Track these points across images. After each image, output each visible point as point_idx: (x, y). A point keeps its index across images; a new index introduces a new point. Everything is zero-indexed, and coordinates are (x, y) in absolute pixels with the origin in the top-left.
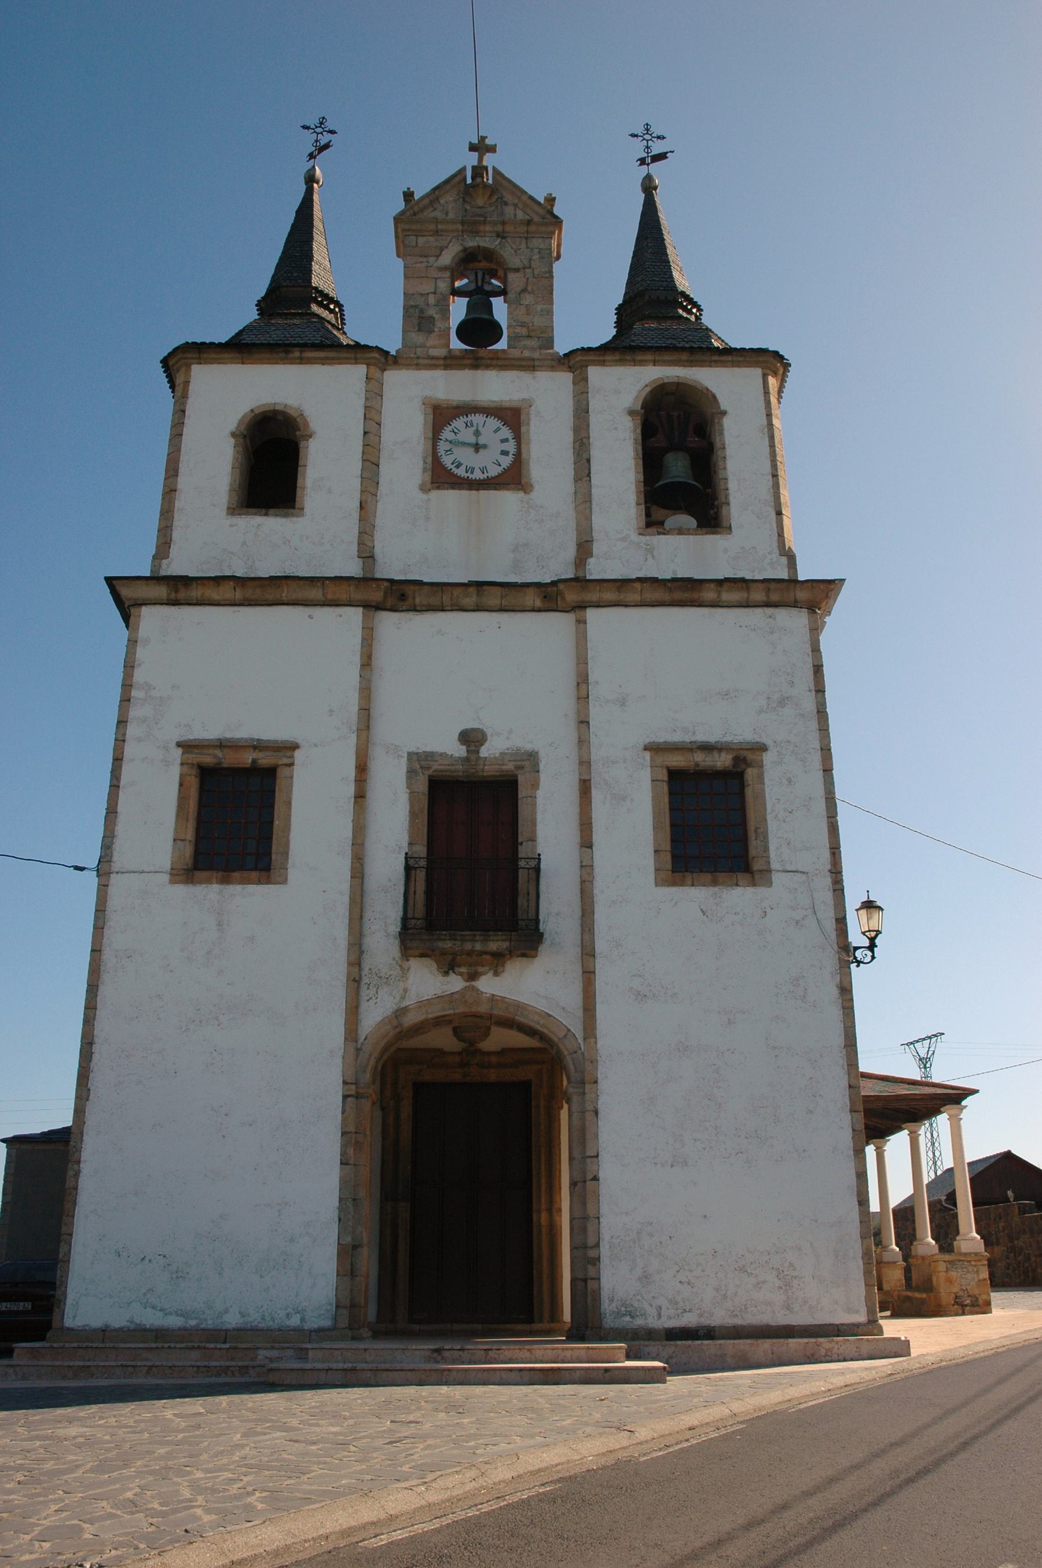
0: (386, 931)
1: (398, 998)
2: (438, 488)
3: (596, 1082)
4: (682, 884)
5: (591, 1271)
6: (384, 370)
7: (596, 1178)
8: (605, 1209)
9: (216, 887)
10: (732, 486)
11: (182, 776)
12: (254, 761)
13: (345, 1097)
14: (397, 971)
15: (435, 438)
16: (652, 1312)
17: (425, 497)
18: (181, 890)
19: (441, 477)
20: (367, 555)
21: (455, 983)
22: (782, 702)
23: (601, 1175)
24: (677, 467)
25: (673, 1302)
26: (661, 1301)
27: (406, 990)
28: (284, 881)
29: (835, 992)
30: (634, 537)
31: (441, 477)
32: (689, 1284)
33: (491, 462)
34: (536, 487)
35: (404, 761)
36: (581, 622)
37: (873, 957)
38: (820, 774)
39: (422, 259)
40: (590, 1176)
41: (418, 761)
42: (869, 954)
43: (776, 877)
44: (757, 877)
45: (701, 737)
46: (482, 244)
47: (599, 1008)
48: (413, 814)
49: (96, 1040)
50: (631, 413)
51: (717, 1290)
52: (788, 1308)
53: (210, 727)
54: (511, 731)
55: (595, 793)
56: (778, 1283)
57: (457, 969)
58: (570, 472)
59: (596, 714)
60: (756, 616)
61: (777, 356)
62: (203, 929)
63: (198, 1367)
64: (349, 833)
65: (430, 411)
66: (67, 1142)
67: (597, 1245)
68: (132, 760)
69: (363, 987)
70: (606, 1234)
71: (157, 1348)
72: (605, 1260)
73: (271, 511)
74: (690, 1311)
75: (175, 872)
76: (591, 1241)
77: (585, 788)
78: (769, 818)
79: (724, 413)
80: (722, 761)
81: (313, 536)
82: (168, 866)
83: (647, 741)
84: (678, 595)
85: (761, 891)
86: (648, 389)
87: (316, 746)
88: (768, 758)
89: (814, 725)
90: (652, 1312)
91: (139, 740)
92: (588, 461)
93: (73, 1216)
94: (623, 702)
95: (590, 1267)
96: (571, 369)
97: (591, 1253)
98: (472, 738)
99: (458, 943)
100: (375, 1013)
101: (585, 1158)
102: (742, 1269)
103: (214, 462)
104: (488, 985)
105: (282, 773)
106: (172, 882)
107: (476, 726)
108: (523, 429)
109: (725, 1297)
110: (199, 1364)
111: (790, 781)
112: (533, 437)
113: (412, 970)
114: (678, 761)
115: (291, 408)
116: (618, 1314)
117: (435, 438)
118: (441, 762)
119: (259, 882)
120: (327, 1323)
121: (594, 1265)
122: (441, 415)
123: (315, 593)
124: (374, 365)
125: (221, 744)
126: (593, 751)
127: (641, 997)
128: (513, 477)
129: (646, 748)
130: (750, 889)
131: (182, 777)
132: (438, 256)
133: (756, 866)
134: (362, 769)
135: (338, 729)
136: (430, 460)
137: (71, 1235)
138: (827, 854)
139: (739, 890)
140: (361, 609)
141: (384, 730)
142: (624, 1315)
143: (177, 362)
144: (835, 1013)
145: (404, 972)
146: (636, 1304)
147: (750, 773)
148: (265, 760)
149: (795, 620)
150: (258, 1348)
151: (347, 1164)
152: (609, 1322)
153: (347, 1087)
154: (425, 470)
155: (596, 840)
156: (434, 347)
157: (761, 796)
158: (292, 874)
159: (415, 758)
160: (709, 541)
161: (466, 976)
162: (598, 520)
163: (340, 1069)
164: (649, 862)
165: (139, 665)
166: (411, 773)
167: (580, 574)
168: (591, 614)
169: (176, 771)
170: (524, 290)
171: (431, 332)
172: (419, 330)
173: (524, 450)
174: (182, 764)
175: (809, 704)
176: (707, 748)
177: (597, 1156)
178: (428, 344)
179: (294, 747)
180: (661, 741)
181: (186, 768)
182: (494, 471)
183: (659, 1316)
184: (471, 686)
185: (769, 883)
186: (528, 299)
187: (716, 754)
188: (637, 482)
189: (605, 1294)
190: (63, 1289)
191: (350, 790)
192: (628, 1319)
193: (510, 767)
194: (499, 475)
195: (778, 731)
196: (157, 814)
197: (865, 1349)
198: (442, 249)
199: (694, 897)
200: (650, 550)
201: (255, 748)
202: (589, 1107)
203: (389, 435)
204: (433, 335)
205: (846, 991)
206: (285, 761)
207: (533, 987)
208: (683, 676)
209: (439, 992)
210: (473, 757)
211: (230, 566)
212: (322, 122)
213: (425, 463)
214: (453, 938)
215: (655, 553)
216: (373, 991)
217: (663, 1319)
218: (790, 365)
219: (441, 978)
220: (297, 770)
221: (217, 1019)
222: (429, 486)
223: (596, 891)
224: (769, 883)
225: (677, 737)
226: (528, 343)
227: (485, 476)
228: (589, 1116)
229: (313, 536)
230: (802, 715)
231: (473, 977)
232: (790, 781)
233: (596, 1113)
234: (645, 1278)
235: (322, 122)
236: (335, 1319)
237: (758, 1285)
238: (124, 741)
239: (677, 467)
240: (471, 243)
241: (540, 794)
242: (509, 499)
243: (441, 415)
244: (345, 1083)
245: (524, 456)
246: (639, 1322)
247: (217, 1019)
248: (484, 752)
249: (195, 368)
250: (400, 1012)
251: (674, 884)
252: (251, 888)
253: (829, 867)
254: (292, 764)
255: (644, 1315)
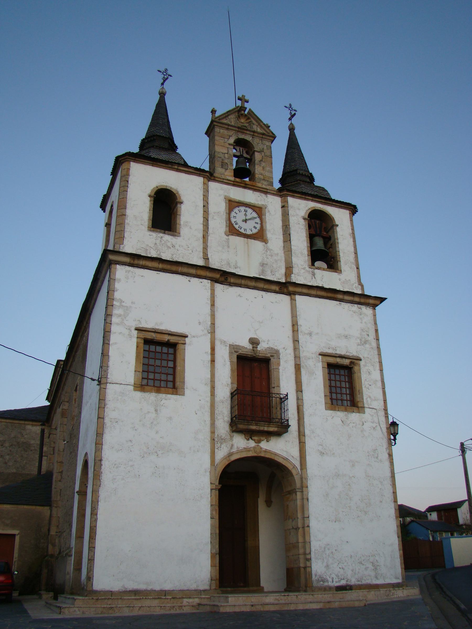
0: (223, 419)
1: (229, 448)
2: (232, 235)
3: (307, 487)
4: (335, 410)
5: (308, 564)
6: (209, 181)
7: (308, 526)
8: (312, 538)
9: (154, 394)
10: (341, 254)
11: (137, 343)
12: (168, 340)
13: (211, 489)
14: (229, 437)
15: (229, 214)
16: (330, 580)
17: (227, 237)
18: (139, 394)
19: (233, 230)
20: (206, 258)
21: (252, 444)
22: (366, 342)
23: (310, 525)
24: (320, 243)
25: (337, 576)
26: (333, 576)
27: (232, 445)
28: (183, 394)
29: (387, 456)
30: (307, 268)
31: (233, 230)
32: (343, 568)
33: (250, 227)
34: (269, 242)
35: (228, 347)
36: (293, 300)
37: (395, 443)
38: (379, 371)
39: (222, 139)
40: (306, 525)
41: (233, 348)
42: (394, 442)
43: (367, 410)
44: (360, 409)
45: (339, 352)
46: (245, 138)
47: (308, 457)
48: (232, 370)
49: (103, 459)
50: (304, 219)
51: (352, 571)
52: (376, 577)
53: (150, 323)
54: (268, 341)
55: (302, 370)
56: (373, 568)
57: (253, 438)
58: (281, 237)
59: (301, 338)
60: (355, 307)
61: (355, 207)
62: (149, 412)
63: (161, 607)
64: (209, 376)
65: (227, 202)
66: (47, 501)
67: (310, 553)
68: (115, 333)
69: (216, 443)
70: (313, 549)
71: (140, 599)
72: (313, 560)
73: (167, 232)
74: (343, 579)
75: (136, 386)
76: (307, 552)
77: (213, 361)
78: (363, 386)
79: (337, 225)
80: (346, 362)
81: (183, 246)
82: (132, 381)
83: (320, 351)
84: (329, 295)
85: (362, 415)
86: (310, 211)
87: (194, 337)
88: (362, 363)
89: (376, 352)
90: (330, 580)
91: (118, 324)
92: (290, 235)
93: (95, 539)
94: (310, 334)
95: (307, 562)
96: (281, 196)
97: (308, 557)
98: (254, 342)
99: (258, 427)
100: (221, 454)
101: (304, 518)
102: (361, 563)
103: (139, 207)
104: (264, 445)
105: (180, 347)
106: (135, 390)
107: (256, 337)
108: (263, 217)
109: (355, 574)
110: (162, 605)
111: (369, 373)
112: (267, 221)
113: (234, 437)
114: (331, 360)
115: (173, 189)
116: (318, 581)
117: (229, 214)
118: (242, 350)
119: (173, 394)
120: (207, 587)
121: (309, 561)
122: (232, 204)
123: (193, 271)
124: (206, 178)
125: (155, 331)
126: (301, 353)
127: (322, 454)
128: (260, 236)
129: (320, 355)
130: (358, 414)
131: (137, 343)
132: (228, 139)
133: (360, 405)
134: (213, 349)
135: (203, 331)
136: (228, 222)
137: (94, 548)
138: (382, 403)
139: (354, 414)
140: (210, 281)
141: (219, 334)
142: (320, 581)
143: (122, 160)
144: (387, 464)
145: (232, 437)
146: (324, 577)
147: (356, 368)
148: (173, 339)
149: (368, 311)
150: (184, 598)
151: (213, 518)
152: (315, 584)
153: (212, 485)
154: (226, 226)
155: (302, 388)
156: (228, 176)
157: (360, 378)
158: (187, 392)
159: (232, 347)
160: (333, 275)
161: (256, 441)
162: (294, 260)
163: (209, 477)
164: (323, 400)
165: (117, 291)
166: (231, 353)
167: (288, 280)
168: (298, 297)
169: (135, 340)
170: (261, 161)
171: (227, 169)
172: (222, 167)
173: (264, 226)
174: (137, 338)
175: (374, 344)
176: (341, 357)
177: (308, 517)
178: (226, 174)
179: (186, 337)
180: (325, 352)
181: (139, 340)
182: (249, 232)
183: (333, 582)
184: (255, 319)
185: (364, 413)
186: (263, 164)
187: (344, 359)
188: (308, 247)
189: (313, 573)
190: (92, 572)
191: (209, 358)
192: (322, 583)
193: (269, 355)
194: (250, 235)
195: (365, 353)
196: (367, 377)
197: (382, 591)
198: (230, 136)
199: (339, 415)
200: (314, 274)
201: (169, 334)
202: (305, 497)
203: (212, 209)
204: (228, 171)
205: (390, 455)
206: (182, 342)
207: (282, 448)
208: (331, 327)
209: (245, 447)
210: (255, 349)
211: (150, 253)
212: (166, 70)
213: (226, 223)
214: (256, 425)
215: (316, 276)
216: (219, 445)
217: (334, 583)
218: (357, 211)
219: (246, 441)
220: (187, 347)
221: (156, 452)
222: (228, 233)
223: (304, 410)
224: (364, 413)
225: (330, 351)
226: (264, 182)
227: (245, 232)
228: (305, 501)
229: (183, 246)
230: (372, 348)
231: (259, 442)
232: (369, 373)
233: (308, 499)
234: (327, 566)
235: (166, 70)
236: (210, 586)
237: (366, 569)
238: (111, 324)
239: (320, 243)
240: (241, 136)
241: (281, 368)
242: (258, 245)
243: (232, 204)
244: (211, 483)
245: (264, 228)
246: (326, 584)
247: (156, 452)
248: (259, 348)
249: (132, 164)
250: (230, 454)
251: (332, 409)
252: (169, 396)
253: (383, 408)
254: (185, 344)
255: (327, 581)
